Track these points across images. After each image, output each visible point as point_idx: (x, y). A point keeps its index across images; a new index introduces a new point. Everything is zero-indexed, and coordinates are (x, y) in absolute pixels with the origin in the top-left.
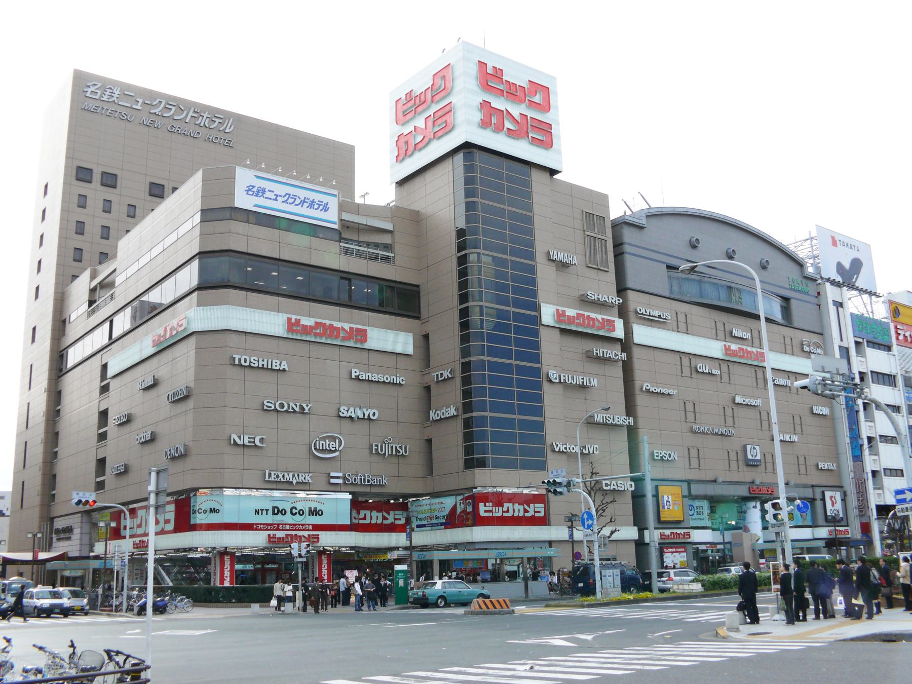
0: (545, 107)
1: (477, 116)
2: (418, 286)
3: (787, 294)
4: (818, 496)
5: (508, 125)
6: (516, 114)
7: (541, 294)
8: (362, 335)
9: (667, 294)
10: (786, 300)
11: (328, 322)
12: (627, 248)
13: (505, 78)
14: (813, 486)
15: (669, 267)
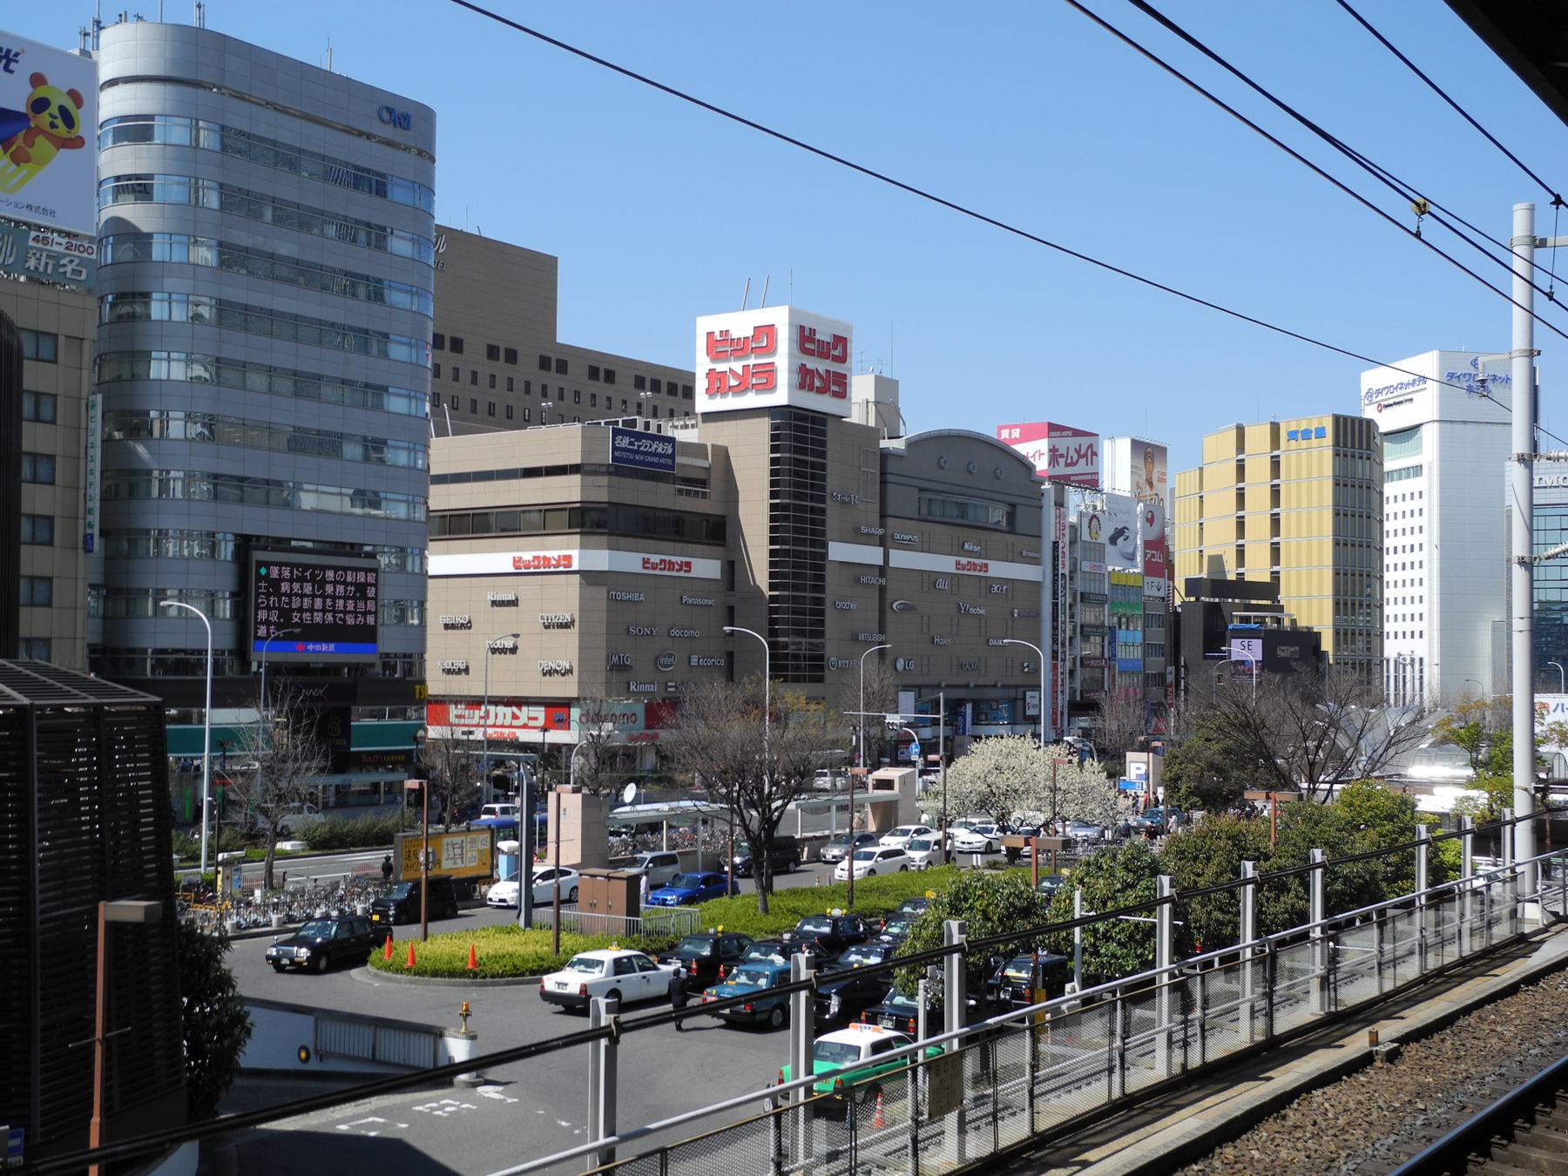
0: (842, 359)
1: (796, 379)
2: (724, 517)
3: (1014, 500)
4: (1020, 696)
5: (817, 383)
6: (822, 370)
7: (829, 534)
8: (688, 564)
9: (916, 516)
10: (1013, 506)
11: (667, 558)
12: (890, 478)
13: (818, 337)
14: (1016, 686)
15: (921, 490)
